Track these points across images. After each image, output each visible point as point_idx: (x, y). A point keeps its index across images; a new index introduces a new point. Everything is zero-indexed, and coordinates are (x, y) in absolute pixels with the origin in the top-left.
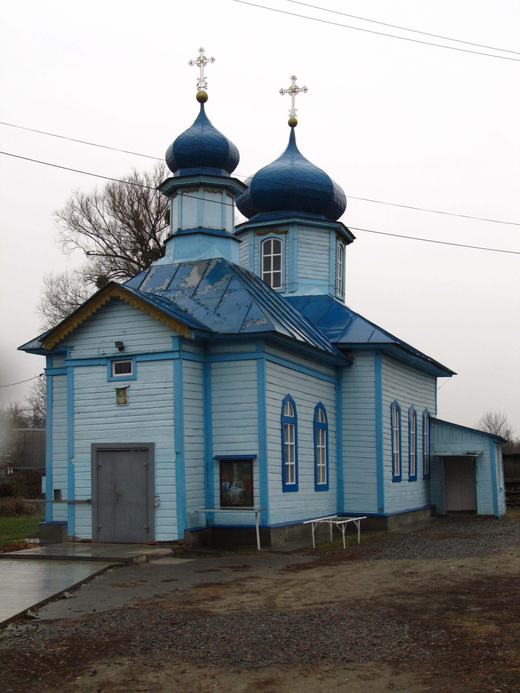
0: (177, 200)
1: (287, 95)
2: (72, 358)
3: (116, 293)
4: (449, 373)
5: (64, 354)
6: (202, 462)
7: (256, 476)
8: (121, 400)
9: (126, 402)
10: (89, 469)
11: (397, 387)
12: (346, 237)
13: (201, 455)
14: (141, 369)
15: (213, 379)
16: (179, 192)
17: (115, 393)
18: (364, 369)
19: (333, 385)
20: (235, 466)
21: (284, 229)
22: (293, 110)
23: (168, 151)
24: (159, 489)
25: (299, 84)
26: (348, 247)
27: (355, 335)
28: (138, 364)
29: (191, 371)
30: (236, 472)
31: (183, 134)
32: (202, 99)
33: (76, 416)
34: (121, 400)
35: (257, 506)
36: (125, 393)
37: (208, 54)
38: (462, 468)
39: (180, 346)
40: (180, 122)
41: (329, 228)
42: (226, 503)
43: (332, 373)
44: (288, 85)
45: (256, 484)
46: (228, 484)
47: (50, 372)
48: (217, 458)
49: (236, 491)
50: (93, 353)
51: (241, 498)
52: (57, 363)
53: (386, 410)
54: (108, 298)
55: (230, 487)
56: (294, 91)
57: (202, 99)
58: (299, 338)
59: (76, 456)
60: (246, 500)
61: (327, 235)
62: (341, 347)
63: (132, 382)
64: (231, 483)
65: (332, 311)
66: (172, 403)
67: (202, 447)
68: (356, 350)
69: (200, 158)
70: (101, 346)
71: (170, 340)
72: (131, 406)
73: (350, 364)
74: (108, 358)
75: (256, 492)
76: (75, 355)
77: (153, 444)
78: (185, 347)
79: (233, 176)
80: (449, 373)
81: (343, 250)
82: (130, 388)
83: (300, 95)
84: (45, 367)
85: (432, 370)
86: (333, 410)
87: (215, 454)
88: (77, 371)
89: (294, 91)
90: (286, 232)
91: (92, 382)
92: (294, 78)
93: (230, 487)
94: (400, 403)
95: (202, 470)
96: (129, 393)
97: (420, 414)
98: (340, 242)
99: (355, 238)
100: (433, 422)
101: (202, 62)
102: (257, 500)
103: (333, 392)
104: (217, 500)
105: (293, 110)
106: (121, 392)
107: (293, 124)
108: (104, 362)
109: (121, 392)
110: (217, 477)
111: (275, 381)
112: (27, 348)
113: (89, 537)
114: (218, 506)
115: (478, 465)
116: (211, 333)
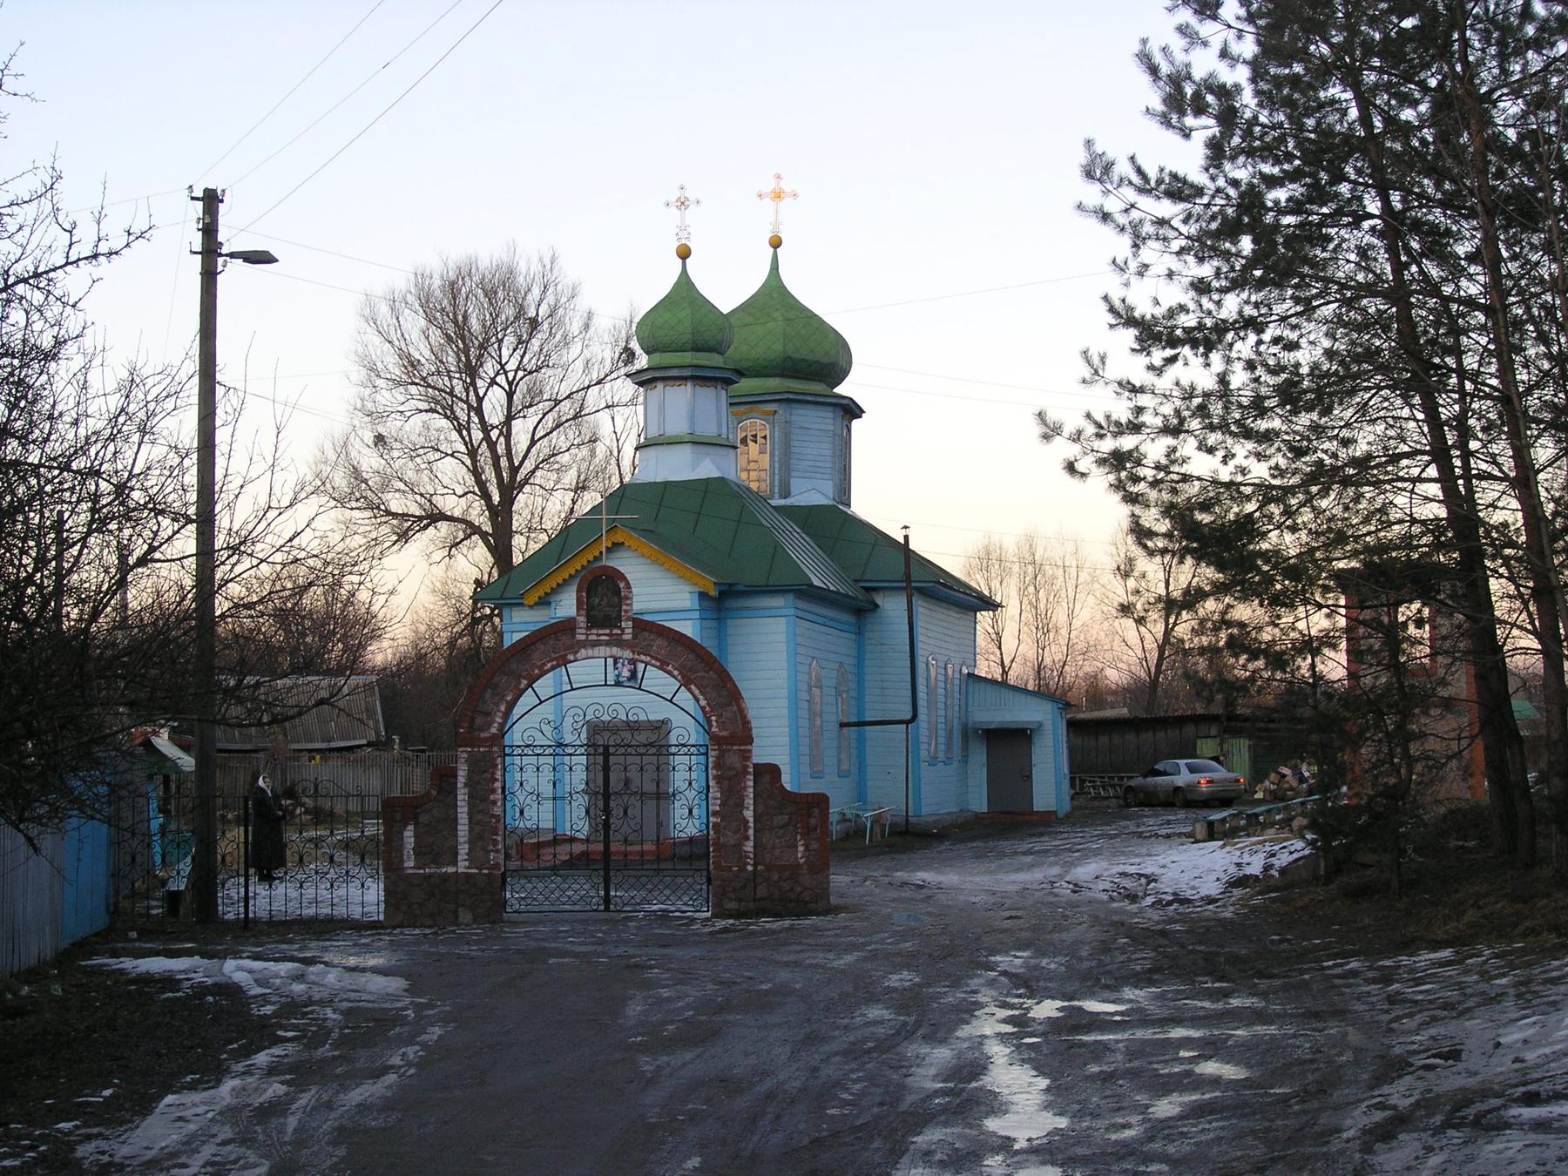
1: (767, 201)
12: (852, 410)
22: (777, 224)
25: (786, 186)
26: (856, 424)
32: (684, 254)
37: (691, 194)
38: (1008, 742)
43: (851, 619)
44: (769, 185)
56: (778, 195)
57: (684, 254)
58: (816, 582)
61: (831, 415)
65: (836, 527)
83: (786, 203)
85: (968, 601)
89: (778, 195)
92: (779, 177)
101: (683, 204)
105: (777, 224)
107: (776, 243)
115: (1035, 740)
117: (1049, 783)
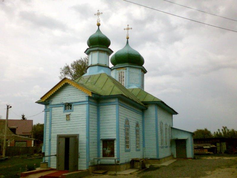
0: (90, 56)
2: (52, 104)
3: (66, 82)
4: (176, 113)
5: (49, 104)
6: (96, 141)
7: (115, 146)
8: (68, 119)
9: (69, 120)
10: (56, 144)
11: (162, 117)
12: (144, 71)
13: (96, 138)
14: (74, 107)
15: (101, 112)
16: (91, 53)
17: (66, 116)
18: (152, 110)
19: (142, 116)
20: (108, 142)
21: (125, 68)
22: (128, 34)
23: (88, 41)
24: (80, 151)
26: (145, 75)
27: (148, 99)
28: (74, 106)
29: (93, 108)
30: (108, 144)
31: (92, 35)
33: (52, 125)
34: (68, 119)
35: (116, 157)
36: (69, 116)
37: (100, 12)
38: (180, 144)
39: (89, 100)
40: (92, 32)
41: (139, 68)
42: (105, 155)
43: (141, 111)
44: (126, 27)
45: (115, 149)
46: (105, 149)
47: (46, 111)
48: (102, 140)
49: (108, 151)
50: (59, 103)
51: (110, 154)
52: (48, 107)
53: (159, 123)
54: (64, 83)
55: (106, 150)
56: (128, 29)
59: (52, 139)
60: (112, 154)
62: (145, 103)
63: (72, 112)
64: (107, 149)
66: (85, 120)
67: (96, 136)
68: (150, 104)
69: (99, 43)
70: (61, 100)
71: (85, 97)
72: (71, 121)
73: (147, 109)
74: (63, 104)
75: (115, 152)
76: (53, 103)
77: (78, 135)
78: (90, 100)
79: (109, 47)
80: (176, 113)
81: (143, 76)
82: (71, 114)
83: (130, 30)
84: (44, 108)
85: (171, 112)
86: (141, 124)
87: (101, 138)
88: (53, 109)
89: (128, 29)
90: (126, 69)
91: (59, 112)
93: (106, 150)
94: (162, 122)
95: (96, 144)
96: (71, 116)
97: (168, 126)
98: (142, 73)
99: (147, 72)
100: (172, 128)
102: (115, 154)
103: (141, 117)
104: (101, 155)
105: (128, 34)
106: (68, 116)
108: (62, 105)
109: (68, 116)
110: (101, 147)
111: (122, 112)
112: (38, 102)
113: (55, 168)
114: (101, 157)
116: (100, 96)
117: (190, 152)
